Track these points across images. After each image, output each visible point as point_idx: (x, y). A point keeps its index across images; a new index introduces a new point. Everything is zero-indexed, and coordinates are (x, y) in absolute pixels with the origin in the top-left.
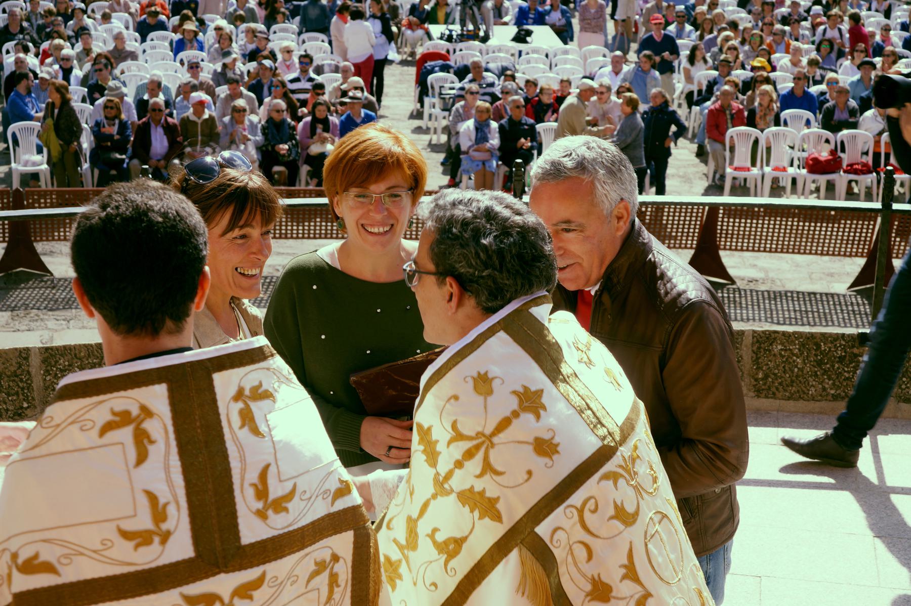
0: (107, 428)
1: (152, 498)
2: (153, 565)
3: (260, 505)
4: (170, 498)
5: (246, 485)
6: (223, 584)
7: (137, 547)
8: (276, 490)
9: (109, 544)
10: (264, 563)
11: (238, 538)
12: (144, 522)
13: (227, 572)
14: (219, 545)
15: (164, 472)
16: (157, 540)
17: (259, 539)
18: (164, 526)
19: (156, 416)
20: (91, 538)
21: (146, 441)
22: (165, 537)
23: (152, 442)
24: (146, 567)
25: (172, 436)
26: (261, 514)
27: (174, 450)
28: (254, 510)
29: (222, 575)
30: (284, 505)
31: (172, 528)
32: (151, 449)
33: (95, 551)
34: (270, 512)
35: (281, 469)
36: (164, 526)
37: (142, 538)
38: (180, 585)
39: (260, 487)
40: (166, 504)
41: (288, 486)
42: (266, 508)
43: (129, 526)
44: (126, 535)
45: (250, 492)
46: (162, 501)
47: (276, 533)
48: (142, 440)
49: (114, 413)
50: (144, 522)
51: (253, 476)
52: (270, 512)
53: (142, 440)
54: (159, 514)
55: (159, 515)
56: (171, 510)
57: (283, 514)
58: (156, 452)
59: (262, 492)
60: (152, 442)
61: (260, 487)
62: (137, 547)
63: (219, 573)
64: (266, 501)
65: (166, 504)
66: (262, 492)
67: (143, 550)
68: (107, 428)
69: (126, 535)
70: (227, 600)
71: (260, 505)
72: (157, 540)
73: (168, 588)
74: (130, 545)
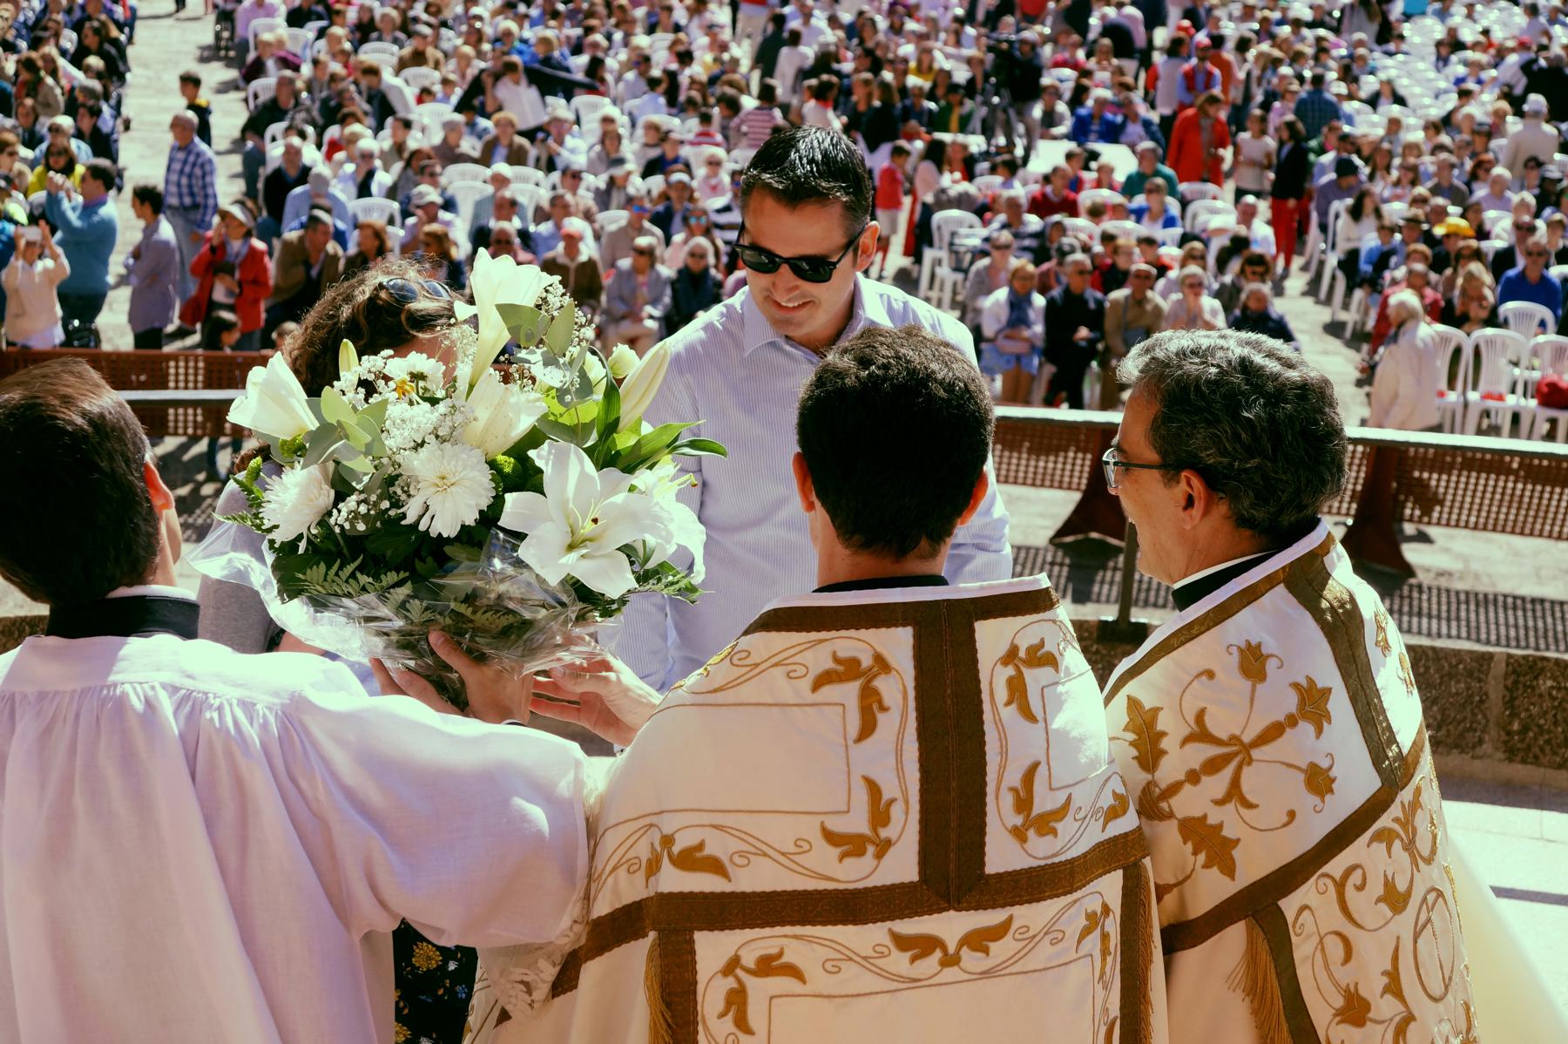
1: (873, 788)
2: (860, 885)
4: (898, 795)
16: (871, 849)
18: (884, 833)
22: (884, 847)
24: (851, 886)
36: (884, 833)
37: (851, 845)
40: (892, 801)
46: (886, 796)
54: (880, 813)
55: (880, 813)
72: (871, 849)
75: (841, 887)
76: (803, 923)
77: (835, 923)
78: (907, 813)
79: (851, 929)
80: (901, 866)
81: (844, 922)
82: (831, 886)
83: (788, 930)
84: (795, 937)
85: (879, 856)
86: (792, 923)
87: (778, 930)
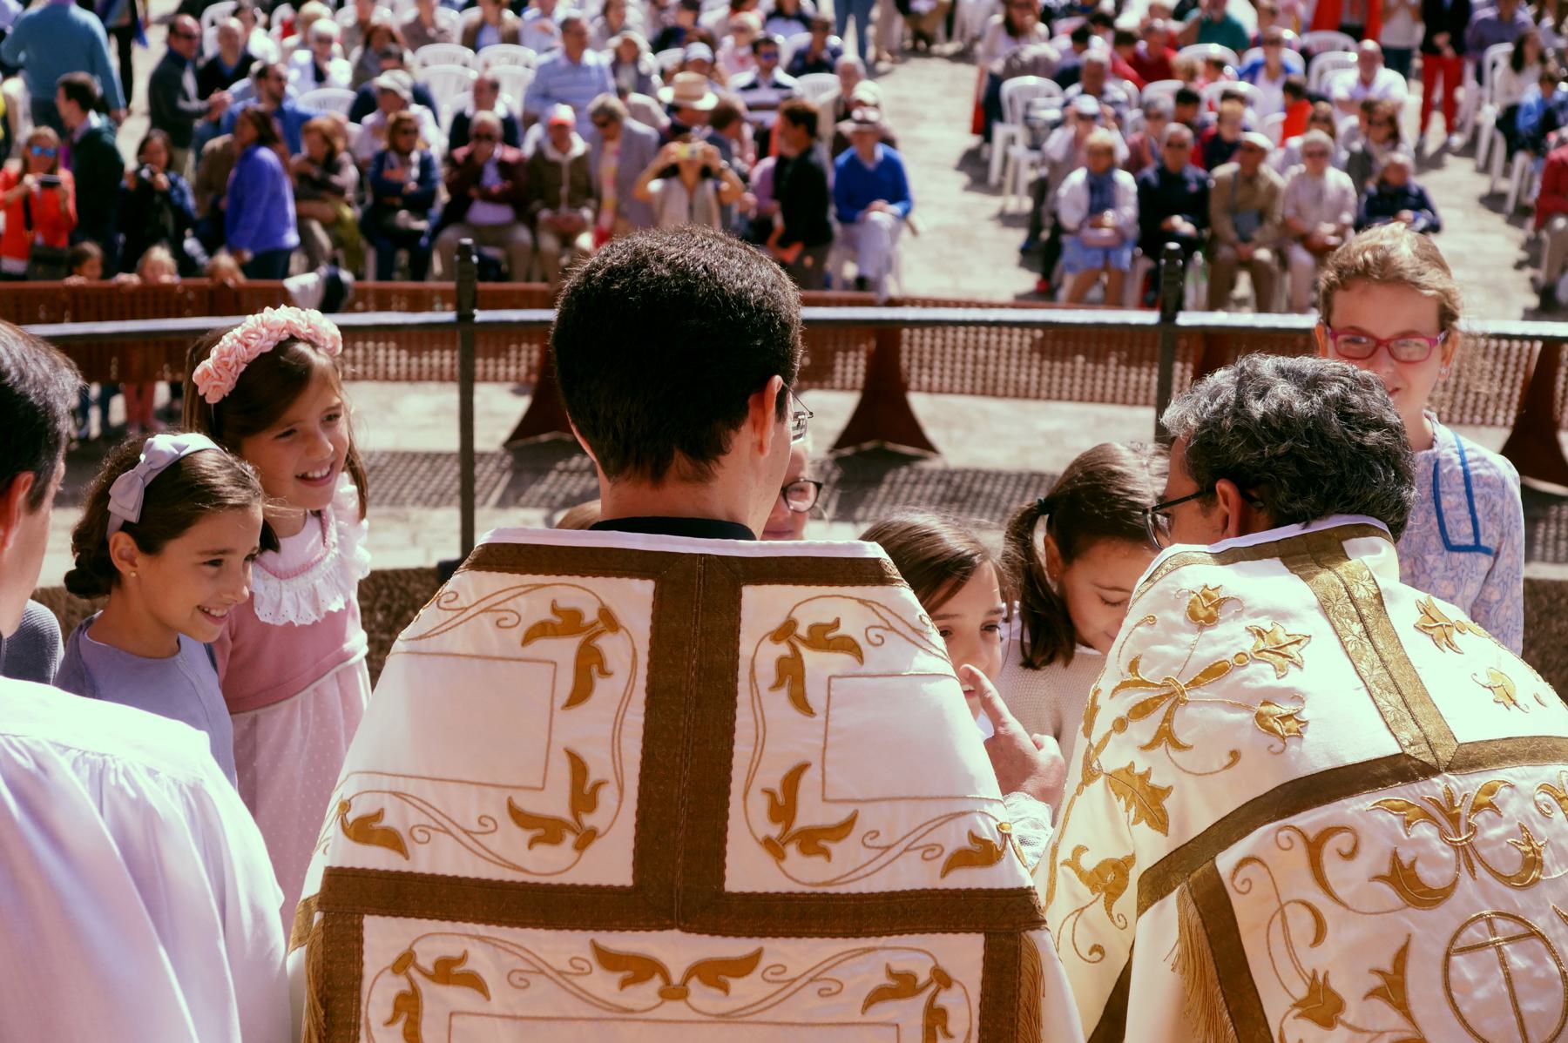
0: (540, 631)
1: (578, 767)
2: (555, 880)
3: (775, 831)
4: (611, 777)
5: (755, 792)
6: (676, 949)
7: (532, 843)
8: (811, 813)
9: (491, 826)
10: (763, 935)
11: (721, 879)
12: (556, 803)
13: (683, 930)
14: (679, 876)
15: (613, 728)
16: (570, 839)
17: (760, 889)
18: (589, 820)
19: (622, 632)
20: (467, 807)
21: (595, 669)
22: (587, 838)
23: (604, 673)
24: (543, 880)
25: (643, 671)
26: (774, 848)
27: (640, 695)
28: (761, 836)
29: (676, 933)
30: (822, 843)
31: (601, 829)
32: (601, 684)
33: (466, 832)
34: (792, 850)
35: (828, 779)
36: (589, 820)
37: (547, 831)
38: (596, 926)
39: (781, 799)
40: (598, 785)
41: (840, 814)
42: (785, 839)
43: (527, 803)
44: (520, 817)
45: (759, 804)
46: (593, 777)
47: (797, 889)
48: (589, 667)
49: (555, 610)
50: (556, 803)
51: (772, 777)
52: (792, 850)
53: (589, 667)
54: (584, 796)
55: (584, 796)
56: (607, 797)
57: (819, 860)
58: (606, 691)
59: (783, 807)
60: (604, 673)
61: (781, 799)
62: (532, 843)
63: (671, 927)
64: (787, 828)
65: (598, 785)
66: (783, 807)
67: (542, 850)
68: (540, 631)
69: (520, 817)
70: (676, 978)
71: (775, 831)
72: (570, 839)
73: (572, 927)
74: (522, 836)
75: (531, 879)
76: (487, 921)
77: (524, 925)
78: (620, 801)
79: (542, 933)
80: (611, 863)
81: (535, 925)
82: (519, 877)
83: (471, 928)
84: (480, 938)
85: (581, 846)
86: (477, 921)
87: (461, 927)
